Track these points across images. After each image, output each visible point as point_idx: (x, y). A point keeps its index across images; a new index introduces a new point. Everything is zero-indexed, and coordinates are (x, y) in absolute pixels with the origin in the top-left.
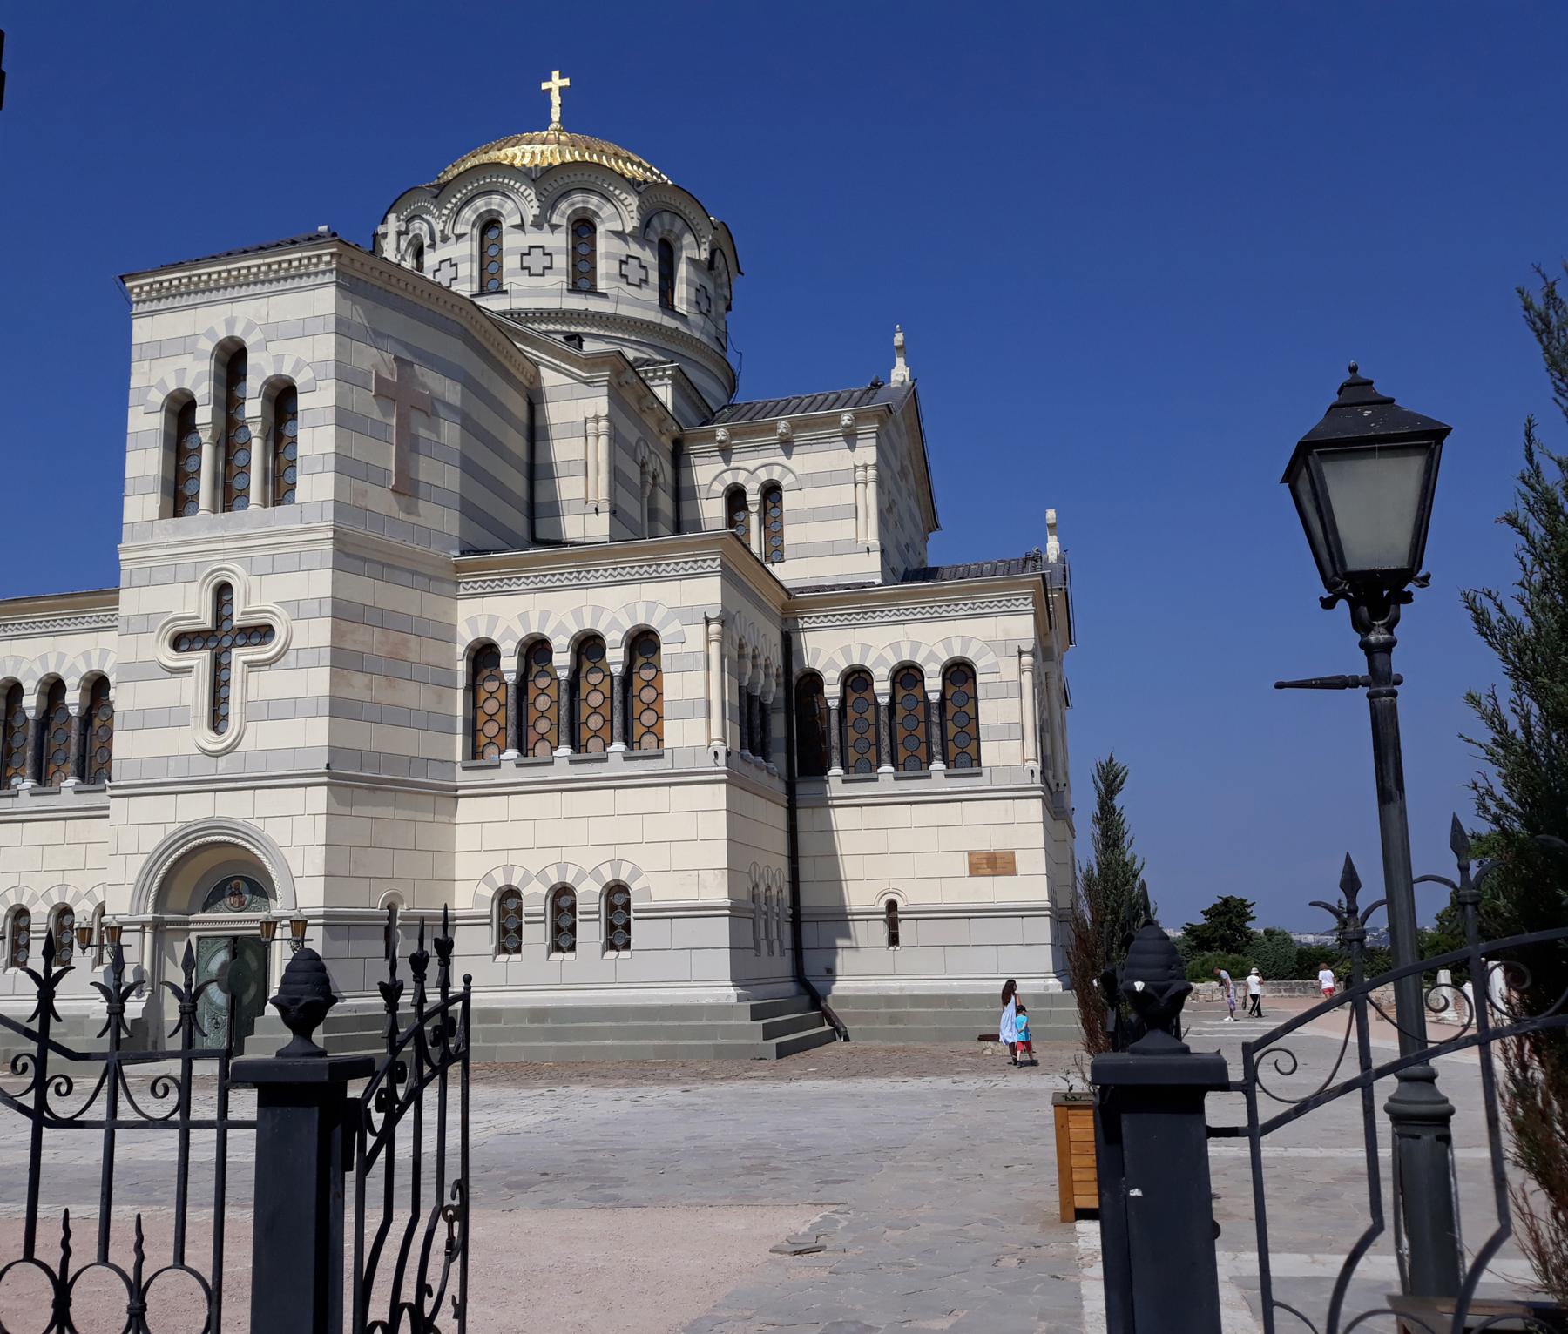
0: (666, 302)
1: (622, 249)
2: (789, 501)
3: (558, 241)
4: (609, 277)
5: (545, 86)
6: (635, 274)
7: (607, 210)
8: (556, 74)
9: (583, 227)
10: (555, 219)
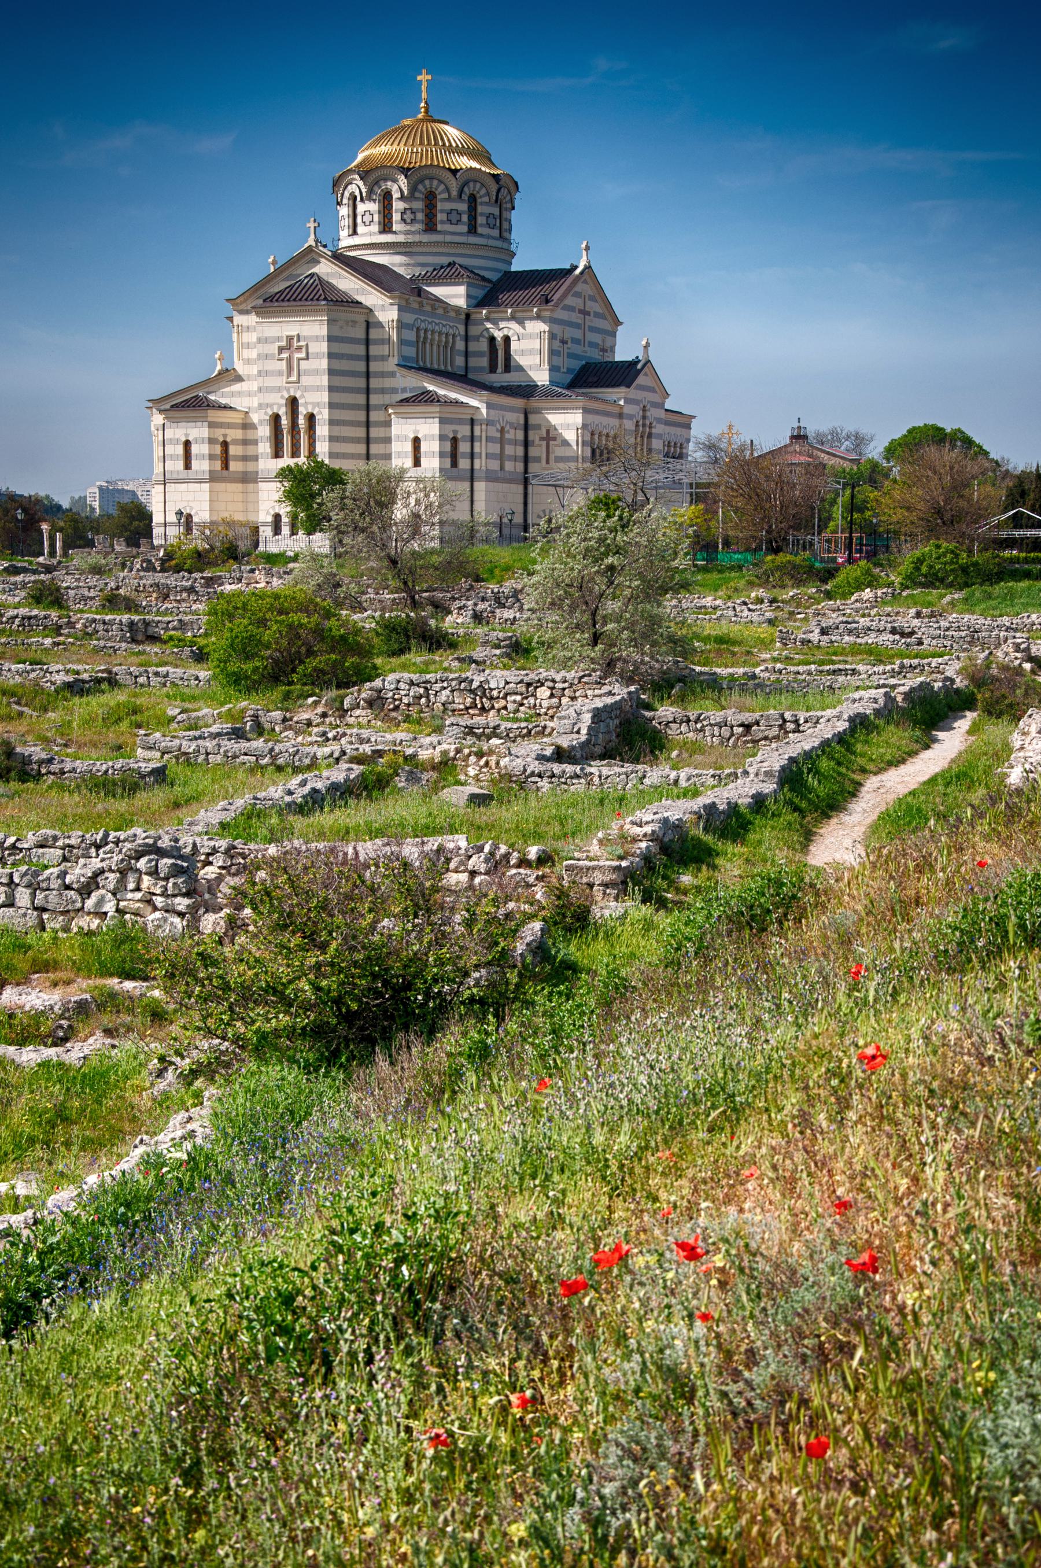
0: (472, 230)
1: (448, 206)
2: (514, 346)
3: (419, 205)
4: (442, 222)
5: (419, 78)
6: (454, 217)
7: (442, 187)
8: (424, 71)
9: (430, 198)
10: (417, 195)
